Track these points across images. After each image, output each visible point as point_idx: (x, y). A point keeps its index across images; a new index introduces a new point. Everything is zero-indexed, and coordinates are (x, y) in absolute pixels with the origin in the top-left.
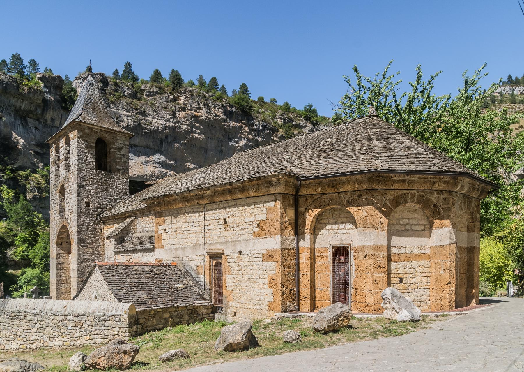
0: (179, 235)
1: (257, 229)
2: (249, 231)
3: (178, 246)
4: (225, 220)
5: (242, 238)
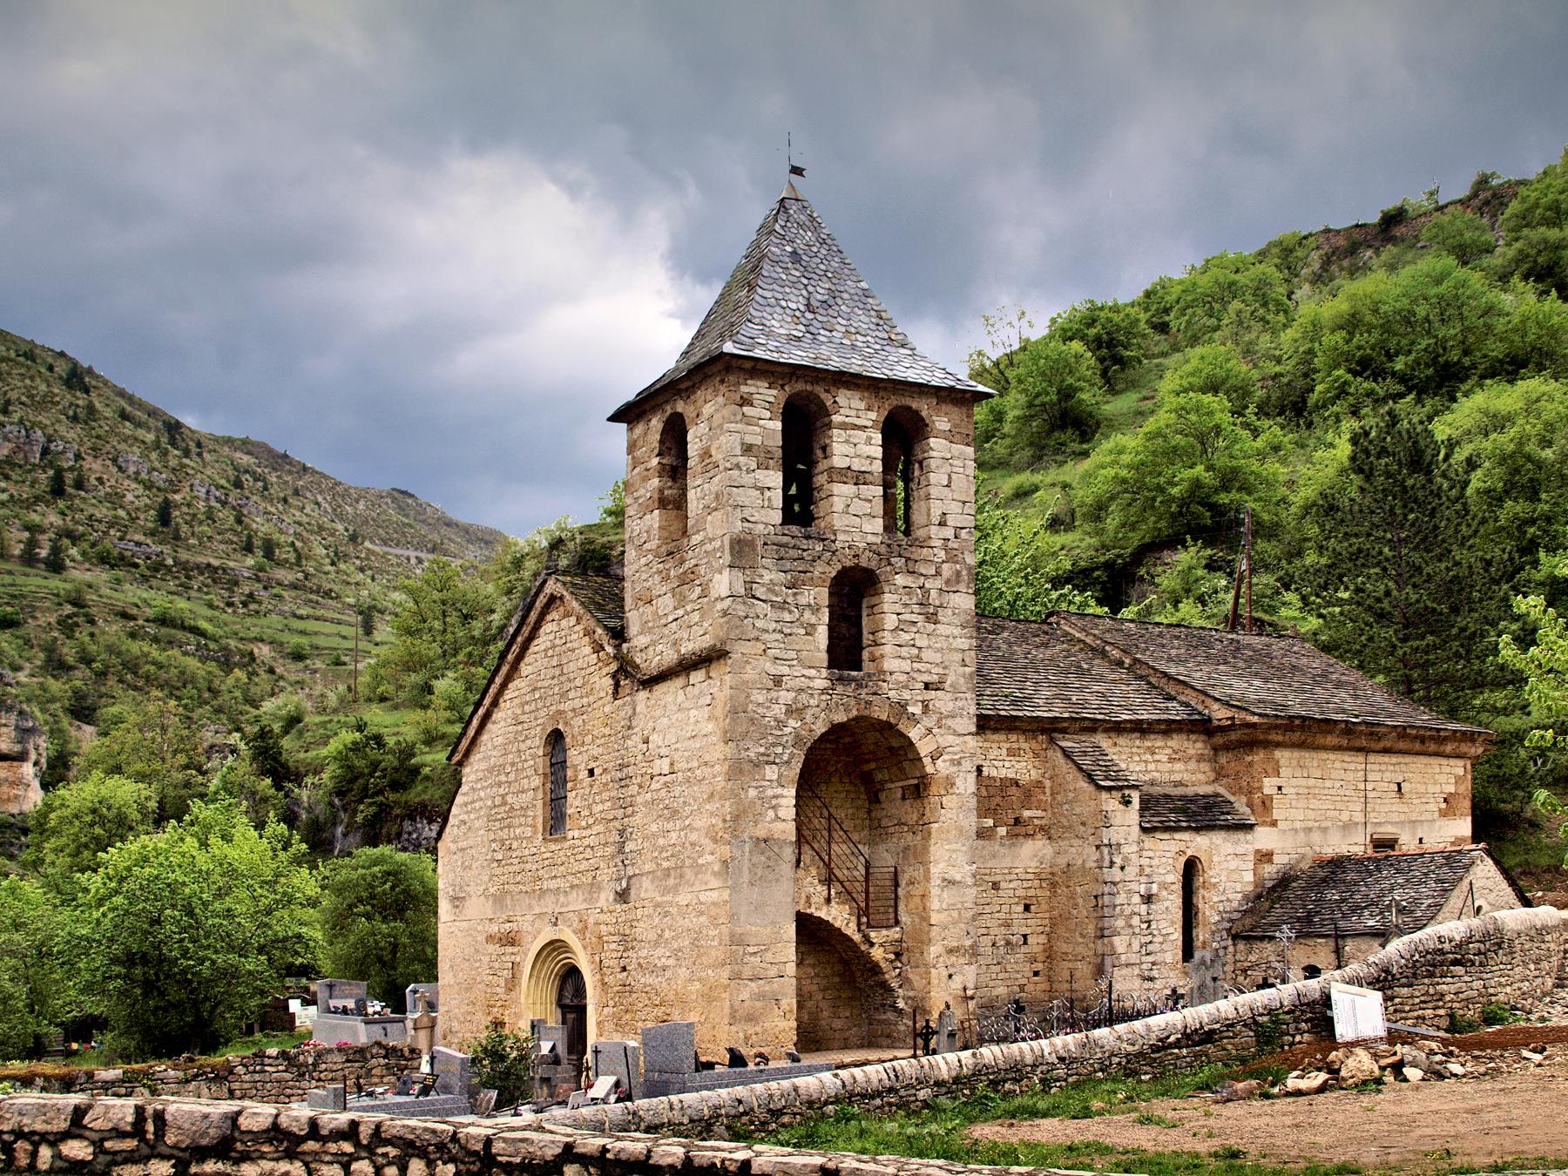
0: (1314, 803)
1: (1444, 806)
2: (1433, 807)
3: (1310, 824)
4: (1399, 784)
5: (1423, 818)
